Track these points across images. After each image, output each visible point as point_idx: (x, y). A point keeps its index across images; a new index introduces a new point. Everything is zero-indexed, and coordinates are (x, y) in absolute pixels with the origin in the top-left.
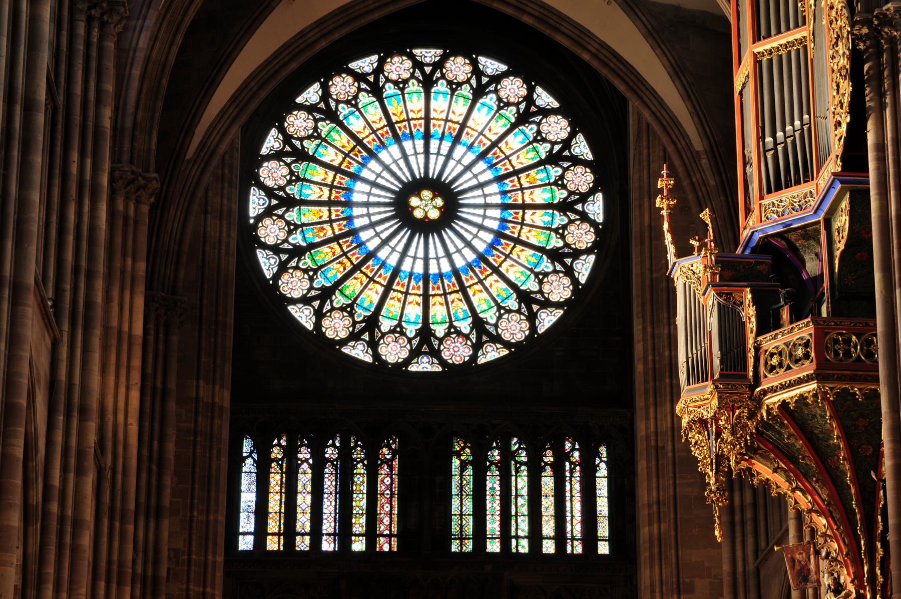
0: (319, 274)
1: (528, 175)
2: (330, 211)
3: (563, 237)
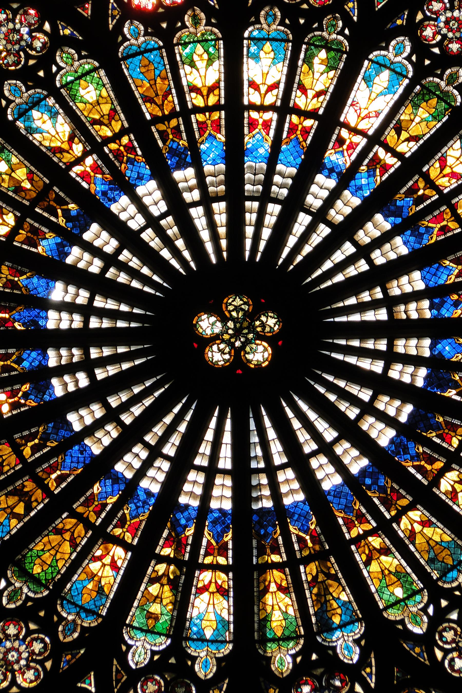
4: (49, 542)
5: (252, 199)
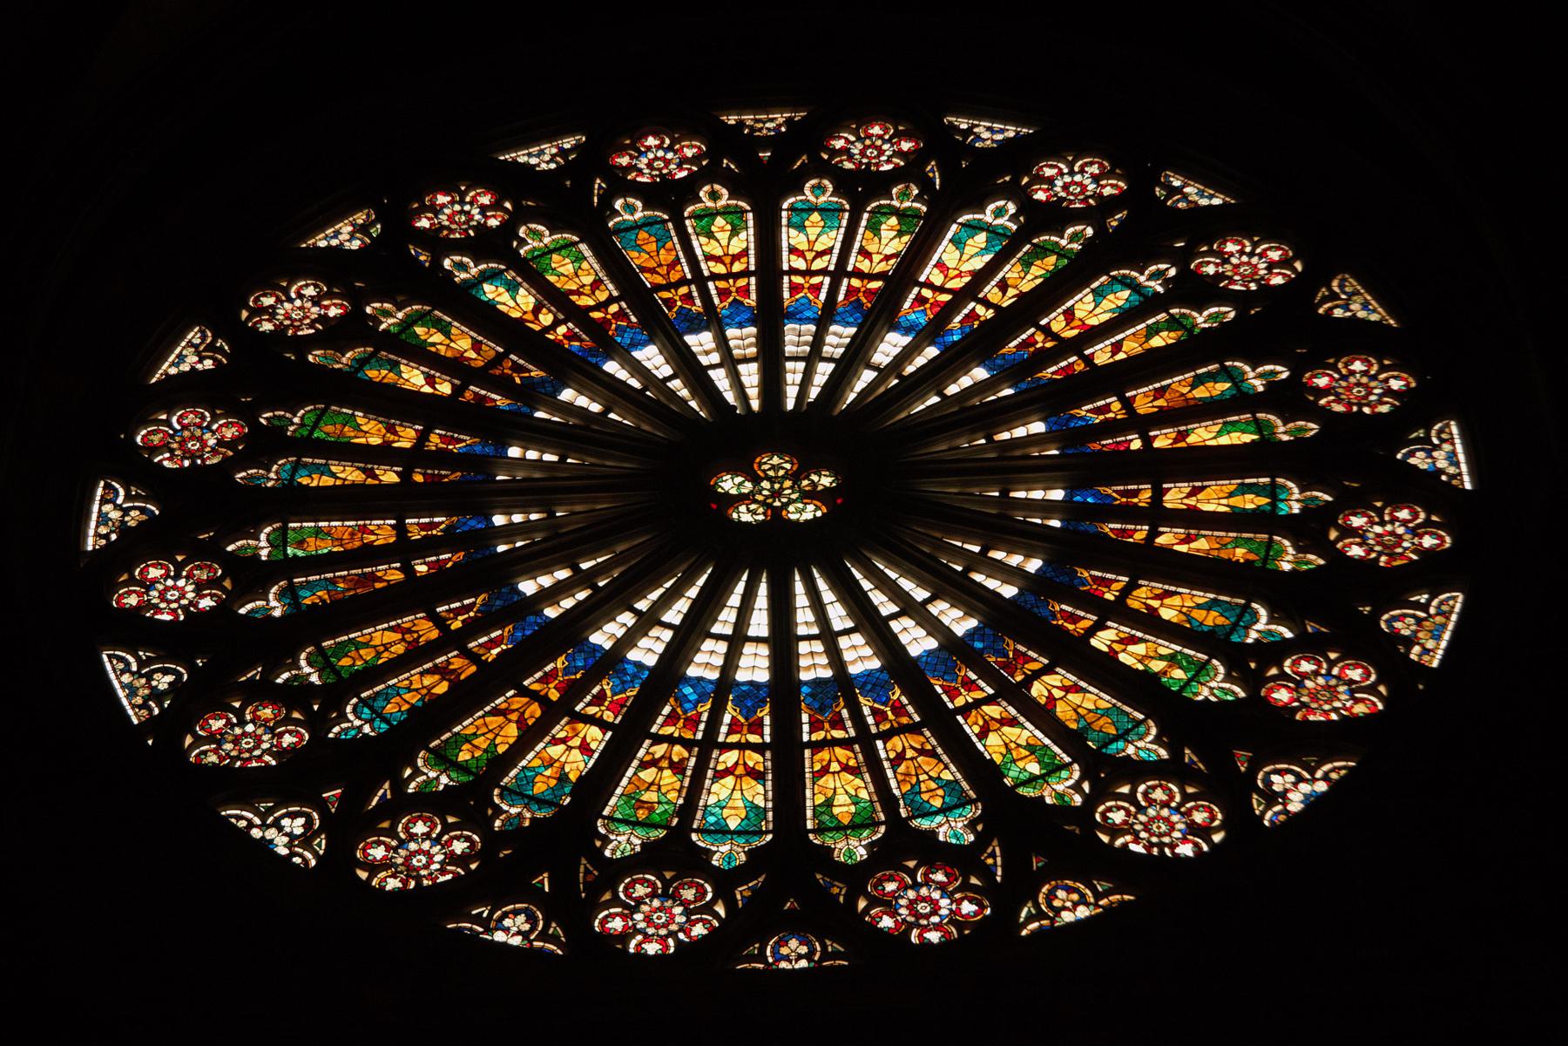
0: (349, 709)
1: (1160, 393)
2: (400, 529)
4: (485, 724)
5: (796, 359)
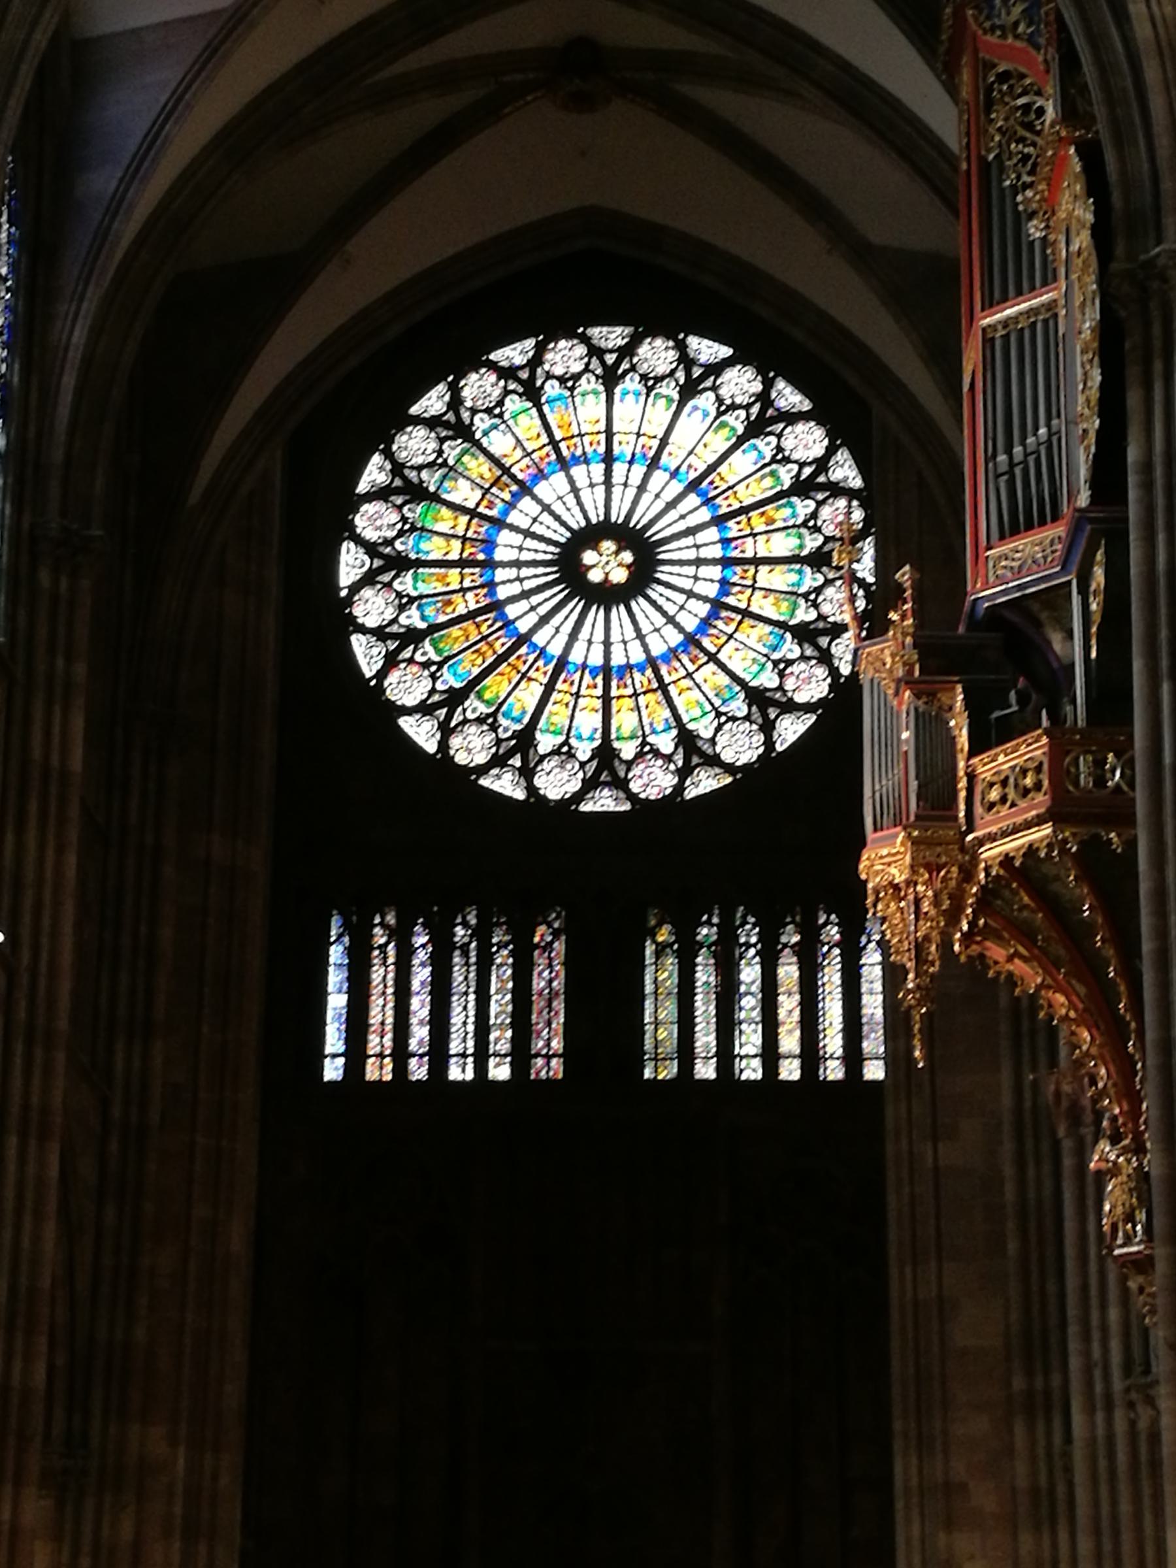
3: (815, 605)
